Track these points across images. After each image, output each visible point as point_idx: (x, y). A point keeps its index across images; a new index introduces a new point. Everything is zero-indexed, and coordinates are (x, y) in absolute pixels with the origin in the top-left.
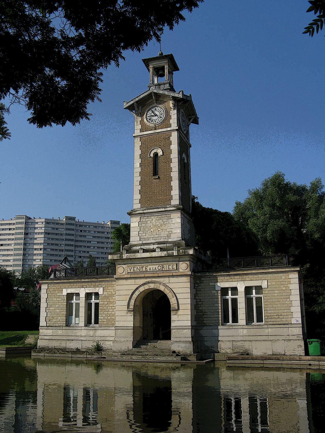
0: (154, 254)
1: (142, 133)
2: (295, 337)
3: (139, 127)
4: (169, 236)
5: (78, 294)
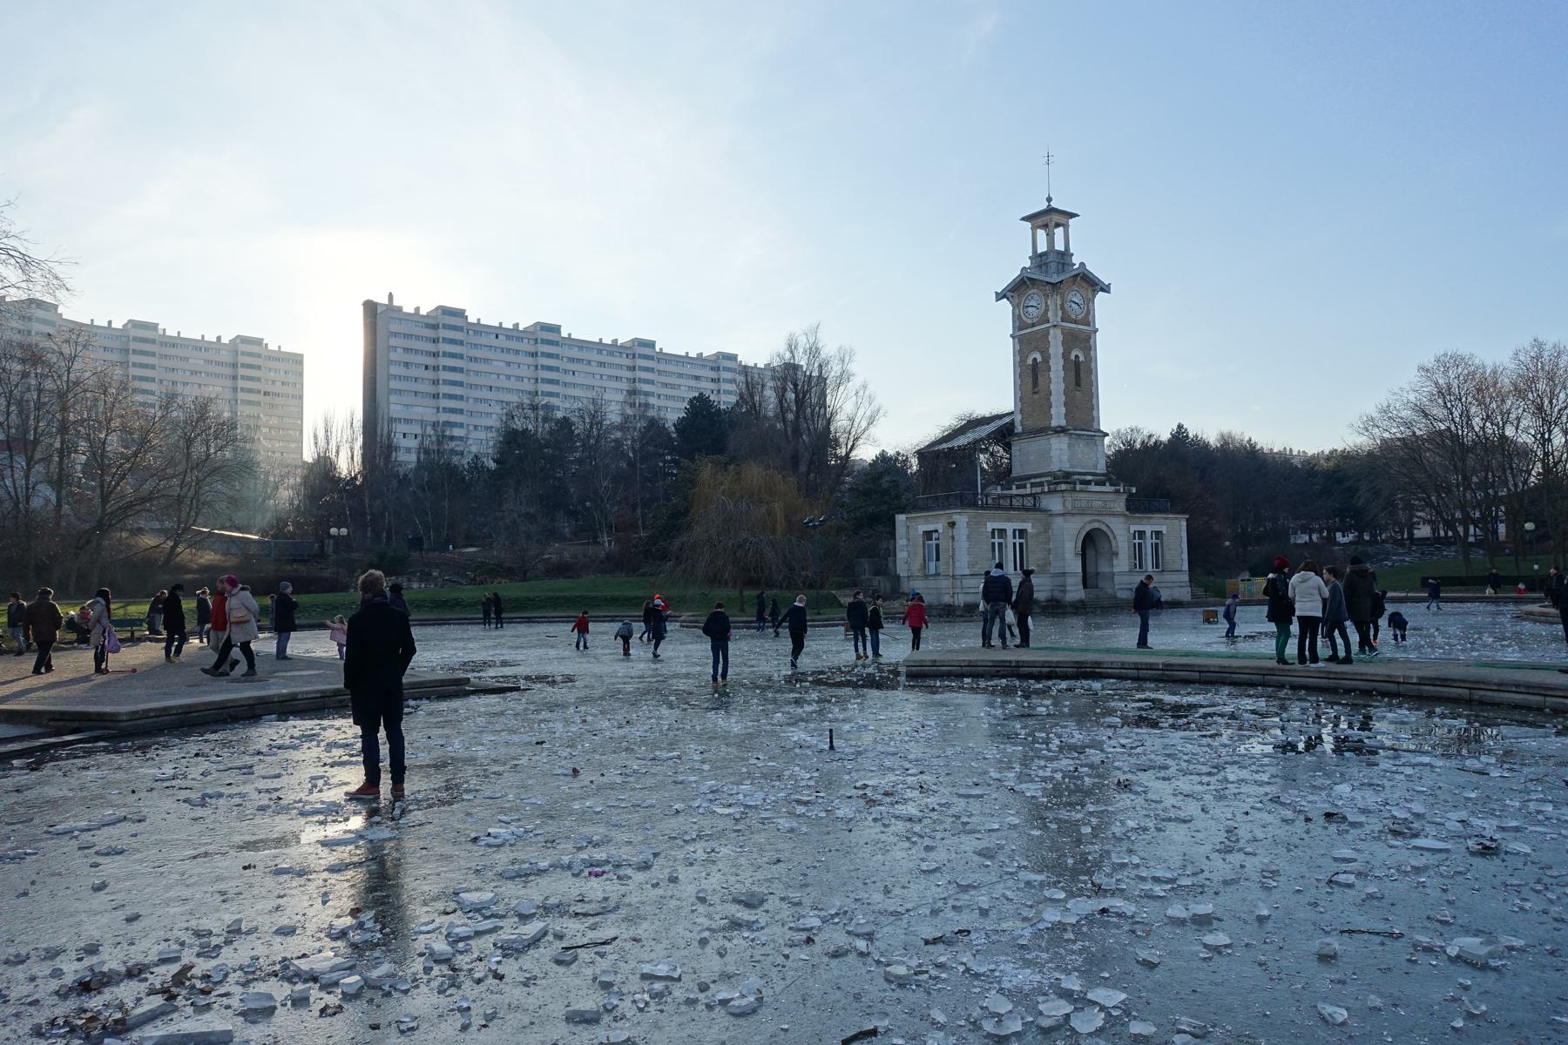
0: (1103, 489)
1: (1064, 324)
2: (1184, 584)
3: (1060, 314)
4: (1095, 467)
5: (1002, 532)
